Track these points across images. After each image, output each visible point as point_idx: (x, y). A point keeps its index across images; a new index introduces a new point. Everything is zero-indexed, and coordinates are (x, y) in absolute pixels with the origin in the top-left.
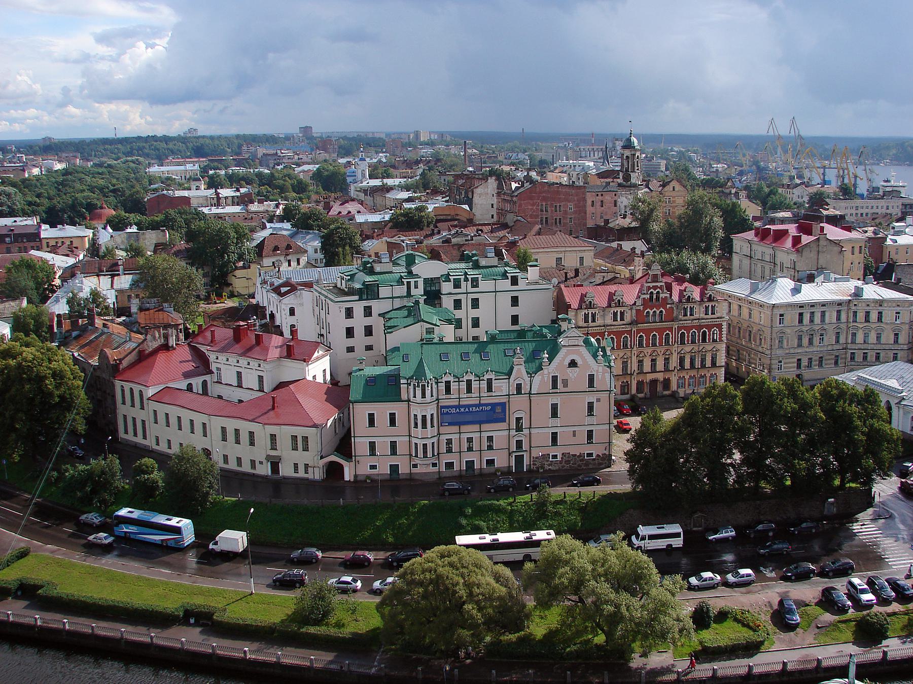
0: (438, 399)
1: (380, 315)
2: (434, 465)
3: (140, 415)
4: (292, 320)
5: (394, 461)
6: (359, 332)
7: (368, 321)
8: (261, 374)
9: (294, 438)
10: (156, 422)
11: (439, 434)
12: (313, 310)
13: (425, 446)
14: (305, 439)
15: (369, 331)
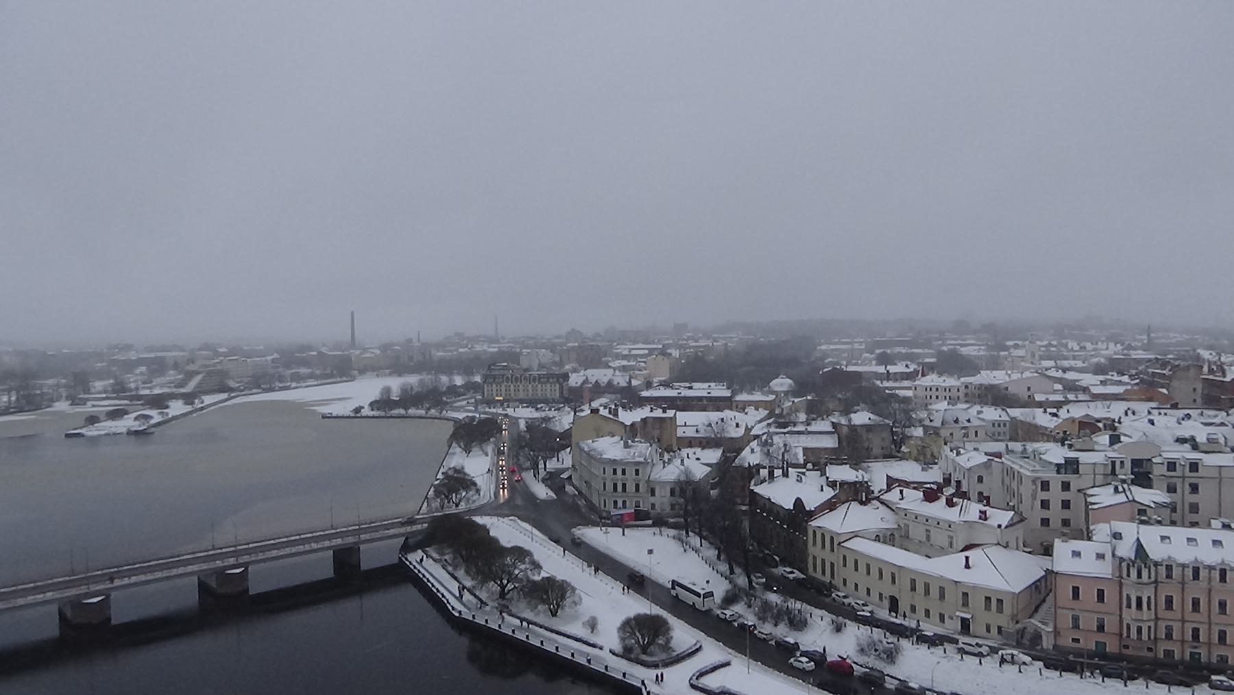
0: (1156, 582)
1: (1079, 491)
2: (1150, 649)
4: (980, 487)
5: (1101, 638)
6: (1056, 505)
7: (1066, 496)
8: (951, 534)
10: (845, 565)
11: (1157, 619)
13: (1139, 630)
15: (1066, 505)
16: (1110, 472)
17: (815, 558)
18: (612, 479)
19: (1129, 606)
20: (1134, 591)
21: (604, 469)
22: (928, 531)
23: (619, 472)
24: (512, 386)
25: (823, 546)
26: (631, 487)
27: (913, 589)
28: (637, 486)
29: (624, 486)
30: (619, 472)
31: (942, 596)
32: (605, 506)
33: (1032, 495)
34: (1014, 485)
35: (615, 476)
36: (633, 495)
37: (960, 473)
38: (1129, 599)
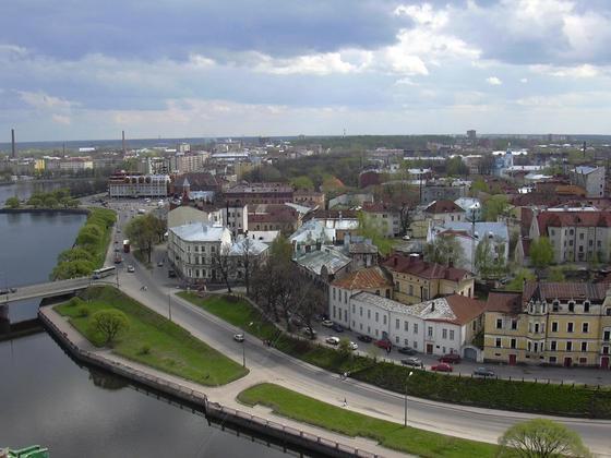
3: (344, 307)
5: (513, 352)
9: (445, 331)
14: (452, 332)
23: (200, 249)
30: (200, 249)
31: (416, 331)
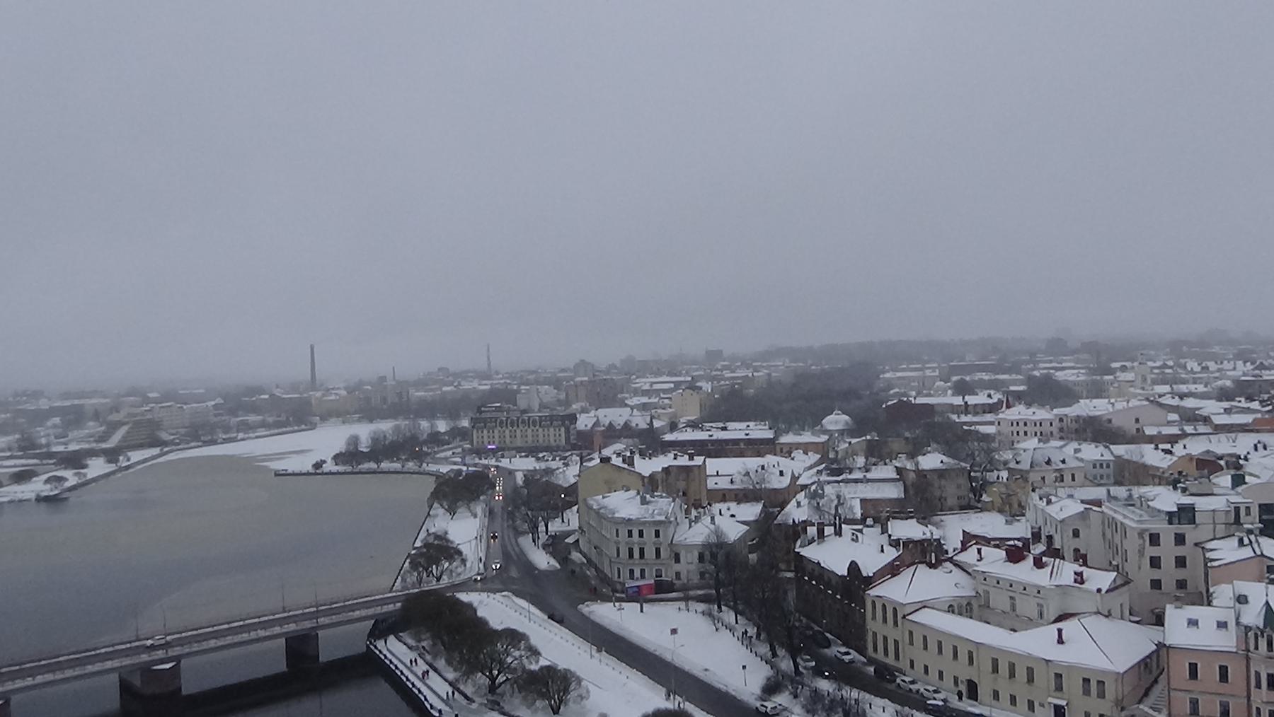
1: (1196, 545)
6: (1168, 562)
7: (1180, 551)
8: (1041, 601)
10: (911, 643)
12: (1104, 534)
15: (1181, 562)
16: (1232, 521)
17: (875, 634)
18: (627, 543)
19: (1259, 686)
20: (1263, 666)
21: (617, 531)
22: (1011, 598)
23: (635, 533)
24: (507, 432)
25: (885, 620)
26: (650, 553)
27: (995, 669)
28: (658, 551)
29: (642, 551)
30: (635, 533)
31: (1031, 680)
32: (619, 577)
33: (1139, 551)
34: (1117, 539)
35: (630, 539)
36: (653, 562)
37: (1051, 525)
38: (1258, 675)
